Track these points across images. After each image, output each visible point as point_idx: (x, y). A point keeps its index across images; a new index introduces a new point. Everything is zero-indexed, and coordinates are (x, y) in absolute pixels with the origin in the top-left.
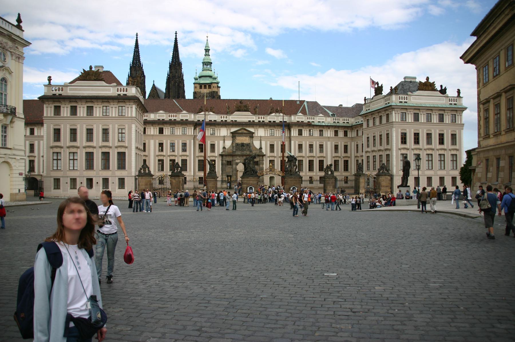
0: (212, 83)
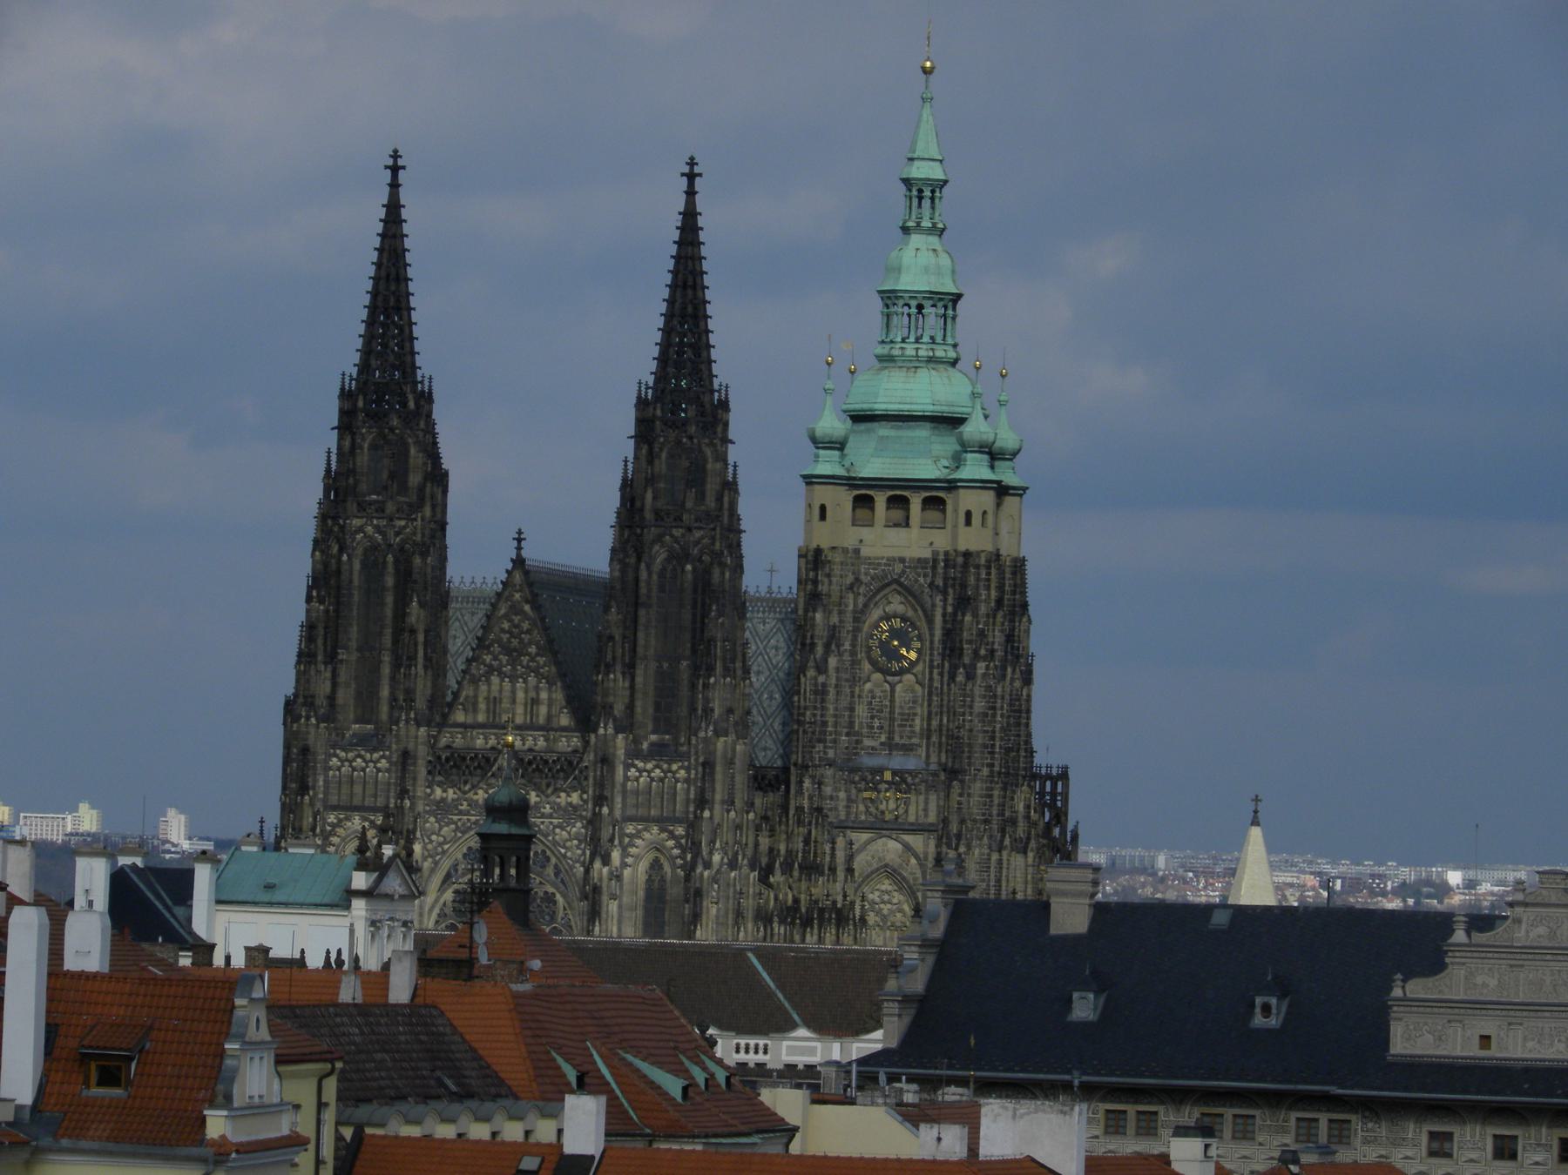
0: (952, 486)
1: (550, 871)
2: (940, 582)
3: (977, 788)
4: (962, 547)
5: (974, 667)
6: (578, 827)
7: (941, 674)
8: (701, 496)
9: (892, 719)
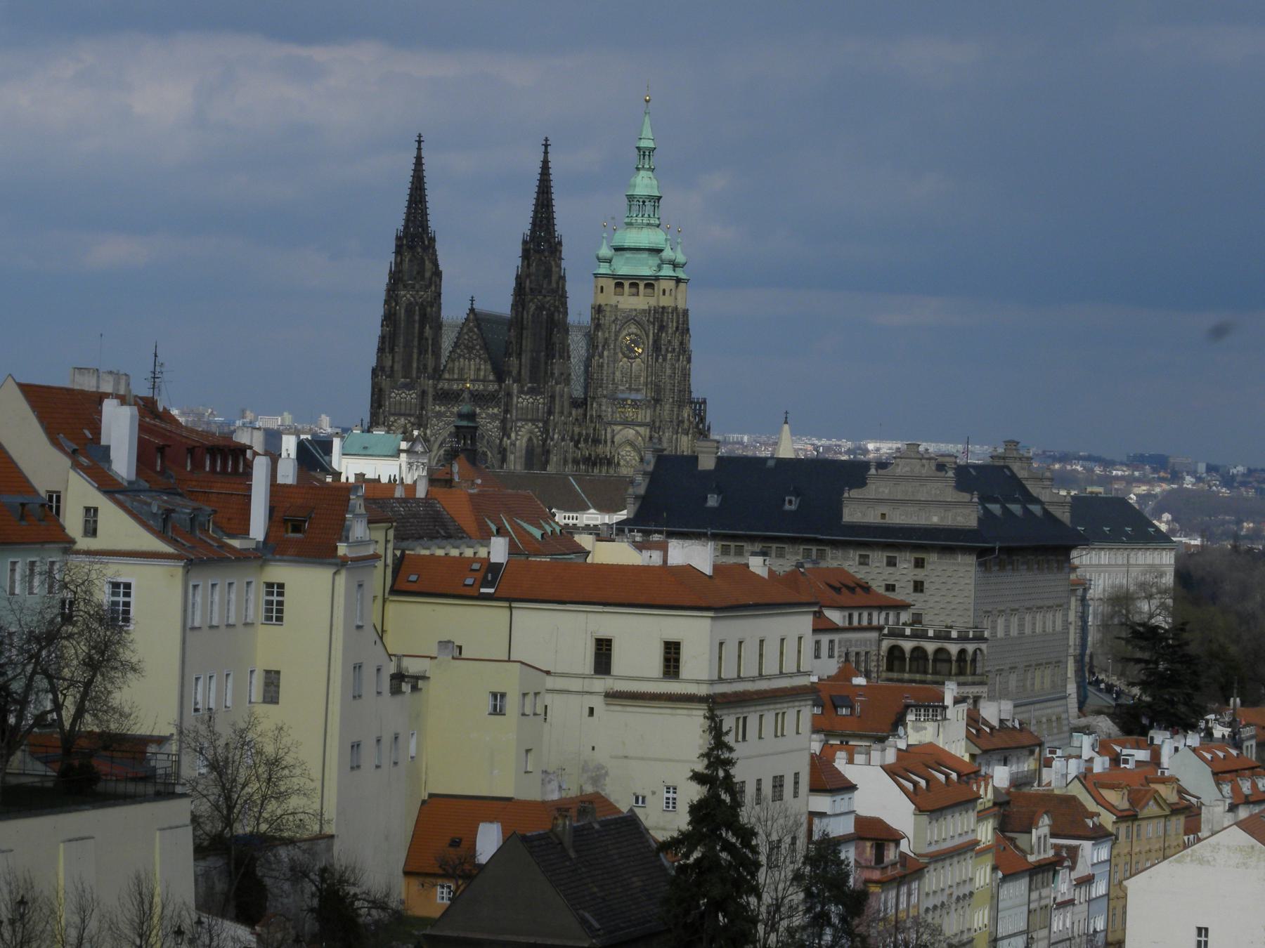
0: (657, 278)
1: (485, 442)
2: (652, 320)
3: (667, 407)
4: (661, 305)
5: (666, 355)
6: (497, 423)
7: (652, 359)
8: (550, 282)
9: (631, 378)
